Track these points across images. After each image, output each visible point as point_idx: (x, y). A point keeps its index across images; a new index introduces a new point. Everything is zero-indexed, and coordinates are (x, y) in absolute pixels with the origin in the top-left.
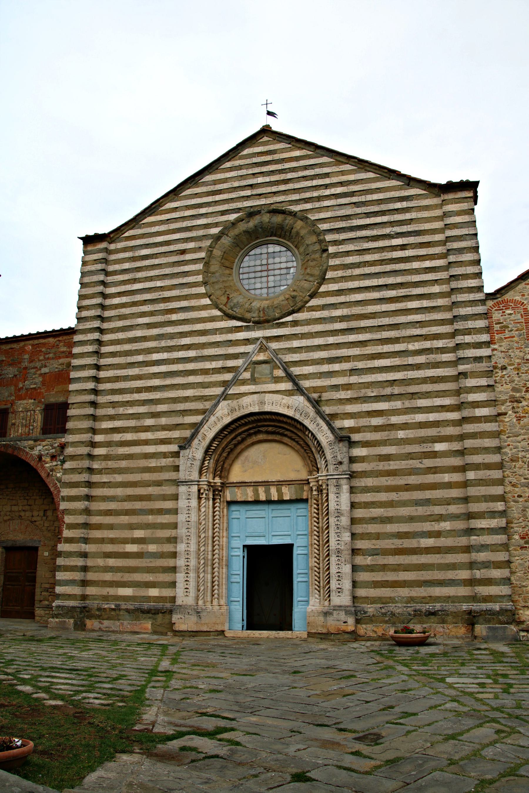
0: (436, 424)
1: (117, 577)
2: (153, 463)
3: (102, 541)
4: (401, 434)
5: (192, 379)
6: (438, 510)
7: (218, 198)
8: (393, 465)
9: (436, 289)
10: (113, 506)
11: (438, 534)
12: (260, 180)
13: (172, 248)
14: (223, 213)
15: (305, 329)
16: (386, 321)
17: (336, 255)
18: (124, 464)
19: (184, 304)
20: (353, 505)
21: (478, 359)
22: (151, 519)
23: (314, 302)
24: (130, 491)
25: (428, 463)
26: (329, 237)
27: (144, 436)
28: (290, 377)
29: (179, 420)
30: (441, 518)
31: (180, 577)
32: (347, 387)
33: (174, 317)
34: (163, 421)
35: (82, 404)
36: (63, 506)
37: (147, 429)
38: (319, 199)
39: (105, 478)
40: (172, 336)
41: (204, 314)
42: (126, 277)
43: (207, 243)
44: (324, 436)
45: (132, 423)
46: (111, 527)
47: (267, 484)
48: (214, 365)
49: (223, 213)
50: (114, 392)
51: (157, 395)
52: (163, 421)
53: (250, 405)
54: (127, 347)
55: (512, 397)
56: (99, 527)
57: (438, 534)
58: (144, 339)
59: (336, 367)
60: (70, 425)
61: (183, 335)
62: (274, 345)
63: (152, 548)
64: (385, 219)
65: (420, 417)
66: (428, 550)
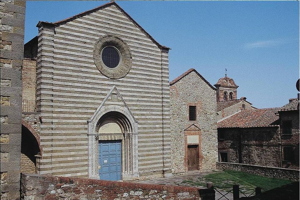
0: (156, 119)
1: (65, 170)
2: (77, 126)
3: (58, 157)
4: (149, 122)
5: (90, 96)
6: (156, 143)
7: (98, 24)
8: (147, 131)
9: (158, 79)
10: (62, 143)
11: (156, 150)
12: (112, 23)
13: (80, 39)
14: (100, 31)
15: (126, 84)
16: (146, 86)
17: (134, 60)
18: (65, 126)
19: (86, 65)
20: (139, 142)
21: (167, 102)
22: (77, 147)
23: (128, 75)
24: (68, 137)
25: (155, 130)
26: (133, 53)
27: (73, 116)
28: (123, 101)
29: (86, 111)
30: (157, 146)
31: (90, 168)
32: (136, 105)
33: (83, 70)
34: (80, 111)
35: (47, 101)
36: (41, 144)
37: (74, 113)
38: (130, 38)
39: (58, 132)
40: (82, 77)
41: (94, 71)
42: (62, 46)
43: (94, 42)
44: (132, 121)
45: (68, 110)
46: (61, 151)
47: (111, 134)
48: (98, 92)
49: (100, 31)
50: (59, 96)
51: (78, 100)
52: (80, 111)
53: (111, 109)
54: (64, 78)
55: (173, 114)
56: (56, 151)
57: (156, 150)
58: (71, 76)
59: (134, 99)
60: (42, 109)
61: (87, 78)
62: (118, 88)
63: (78, 158)
64: (147, 52)
65: (153, 117)
66: (154, 155)
